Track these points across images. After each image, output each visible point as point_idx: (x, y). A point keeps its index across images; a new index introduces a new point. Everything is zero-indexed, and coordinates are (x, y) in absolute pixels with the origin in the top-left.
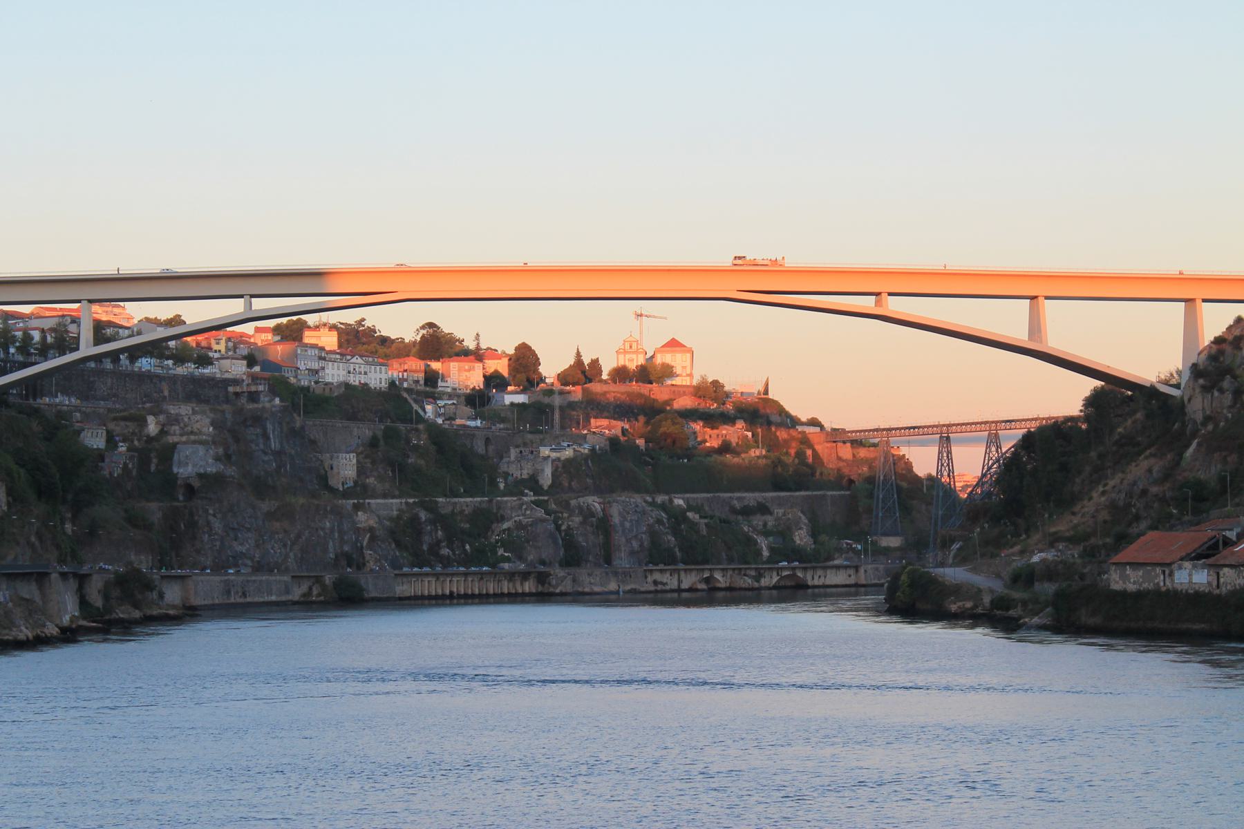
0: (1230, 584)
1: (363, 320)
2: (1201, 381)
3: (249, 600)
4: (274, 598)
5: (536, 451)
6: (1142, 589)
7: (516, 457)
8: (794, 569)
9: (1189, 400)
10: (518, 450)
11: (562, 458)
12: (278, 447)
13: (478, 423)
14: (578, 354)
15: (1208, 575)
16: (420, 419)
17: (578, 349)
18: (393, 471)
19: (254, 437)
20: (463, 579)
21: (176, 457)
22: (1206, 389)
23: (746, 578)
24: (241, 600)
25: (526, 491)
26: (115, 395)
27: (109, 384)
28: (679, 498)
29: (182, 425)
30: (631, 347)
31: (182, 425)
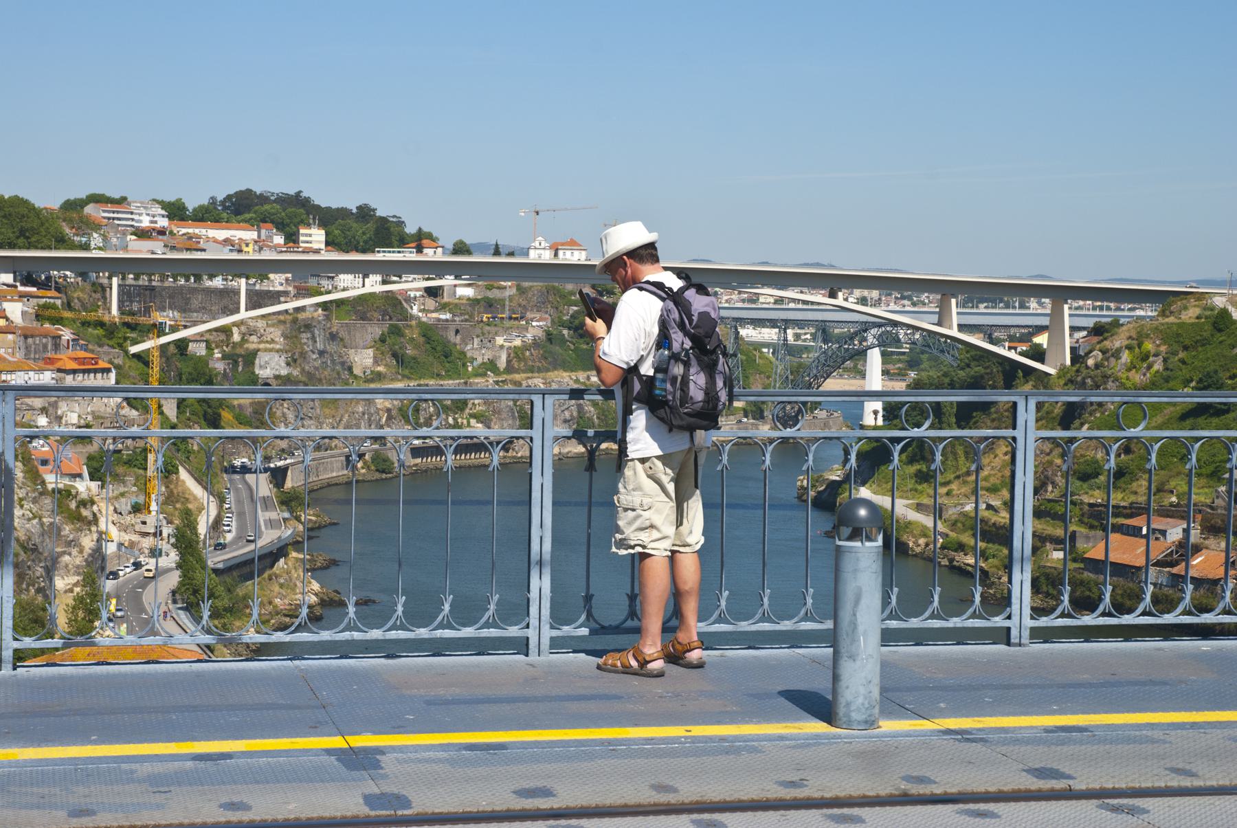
1: (300, 192)
3: (320, 478)
4: (334, 474)
7: (478, 345)
10: (479, 339)
12: (322, 347)
14: (497, 245)
16: (412, 317)
18: (398, 362)
19: (305, 341)
21: (257, 362)
24: (317, 479)
25: (489, 373)
26: (204, 308)
27: (200, 300)
29: (259, 335)
31: (259, 335)
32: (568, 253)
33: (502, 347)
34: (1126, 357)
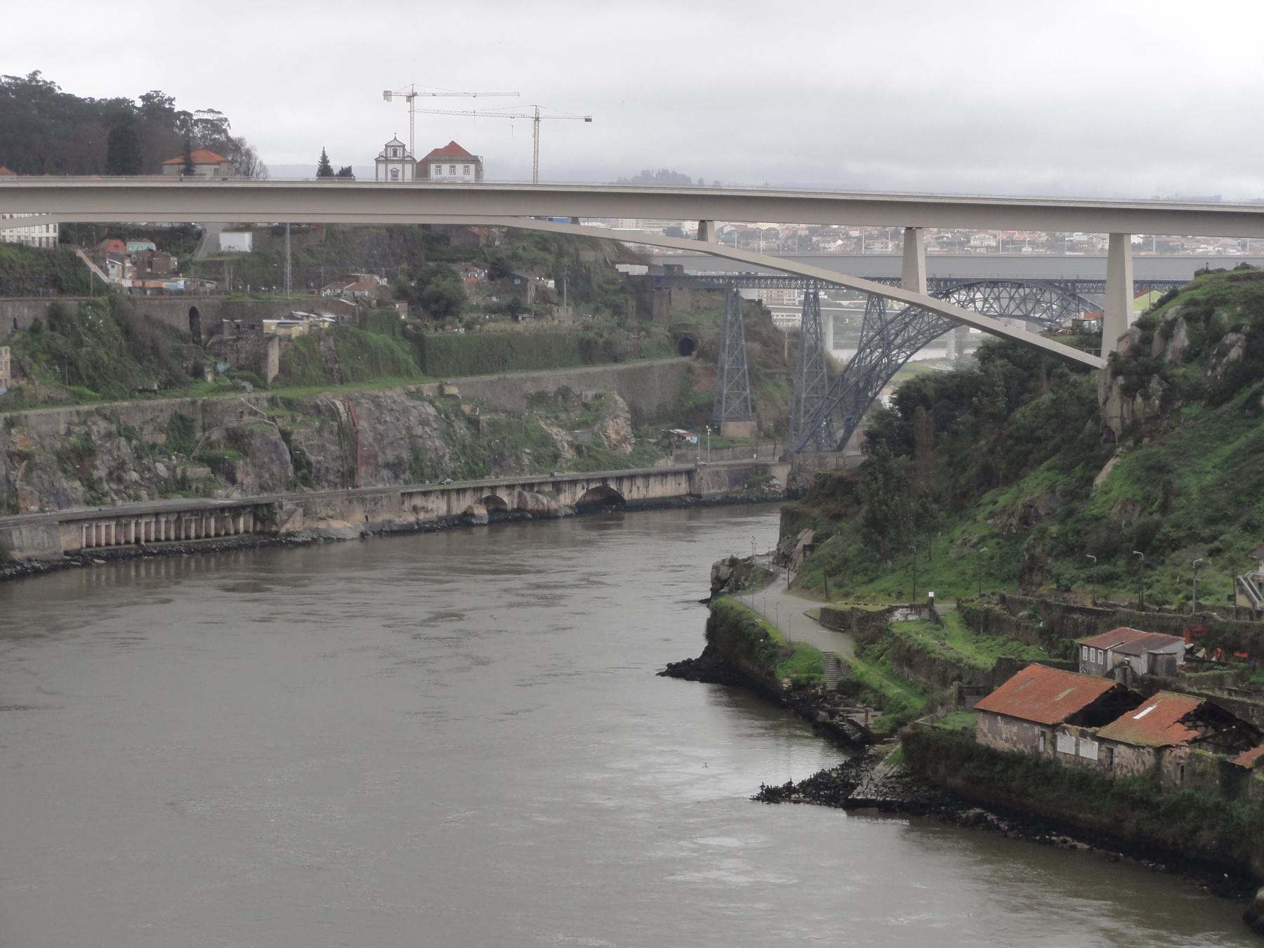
0: (1126, 767)
2: (1121, 380)
5: (259, 326)
6: (1016, 750)
8: (604, 480)
9: (1105, 403)
11: (293, 336)
13: (181, 284)
14: (324, 159)
15: (1099, 750)
16: (103, 289)
17: (324, 152)
20: (154, 520)
22: (1128, 392)
23: (540, 496)
28: (451, 385)
30: (395, 153)
32: (446, 168)
33: (271, 338)
34: (1182, 338)
